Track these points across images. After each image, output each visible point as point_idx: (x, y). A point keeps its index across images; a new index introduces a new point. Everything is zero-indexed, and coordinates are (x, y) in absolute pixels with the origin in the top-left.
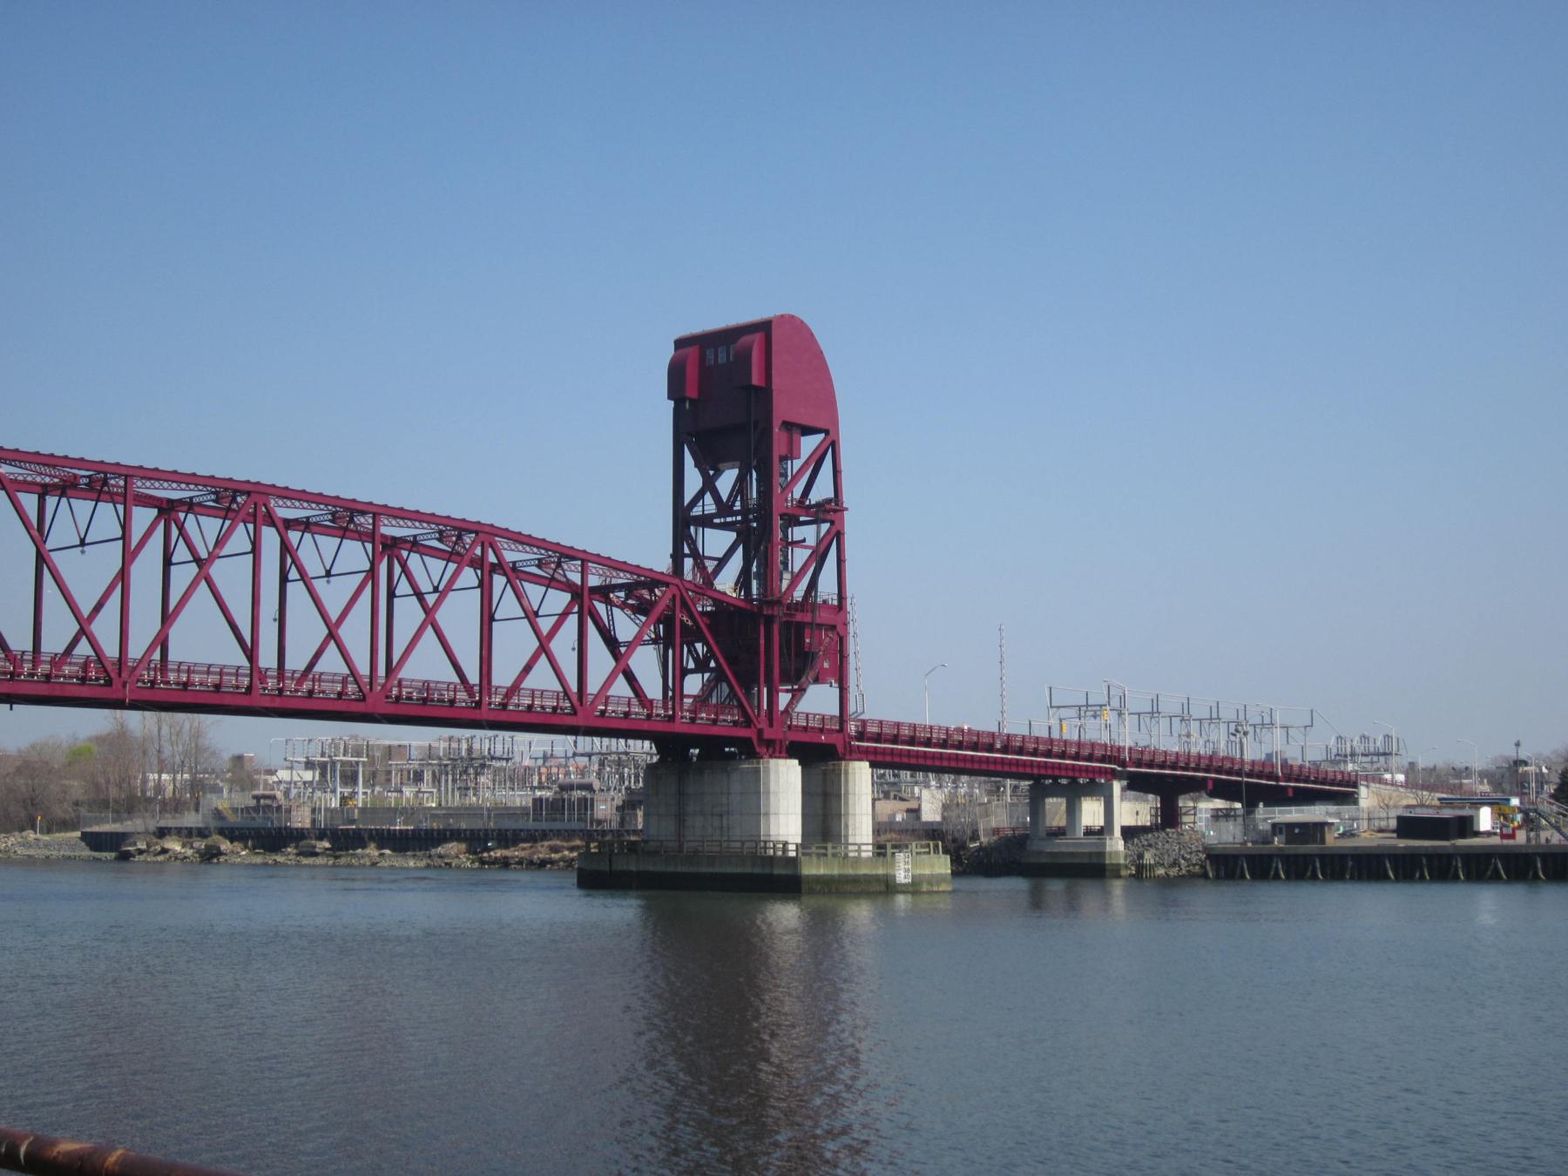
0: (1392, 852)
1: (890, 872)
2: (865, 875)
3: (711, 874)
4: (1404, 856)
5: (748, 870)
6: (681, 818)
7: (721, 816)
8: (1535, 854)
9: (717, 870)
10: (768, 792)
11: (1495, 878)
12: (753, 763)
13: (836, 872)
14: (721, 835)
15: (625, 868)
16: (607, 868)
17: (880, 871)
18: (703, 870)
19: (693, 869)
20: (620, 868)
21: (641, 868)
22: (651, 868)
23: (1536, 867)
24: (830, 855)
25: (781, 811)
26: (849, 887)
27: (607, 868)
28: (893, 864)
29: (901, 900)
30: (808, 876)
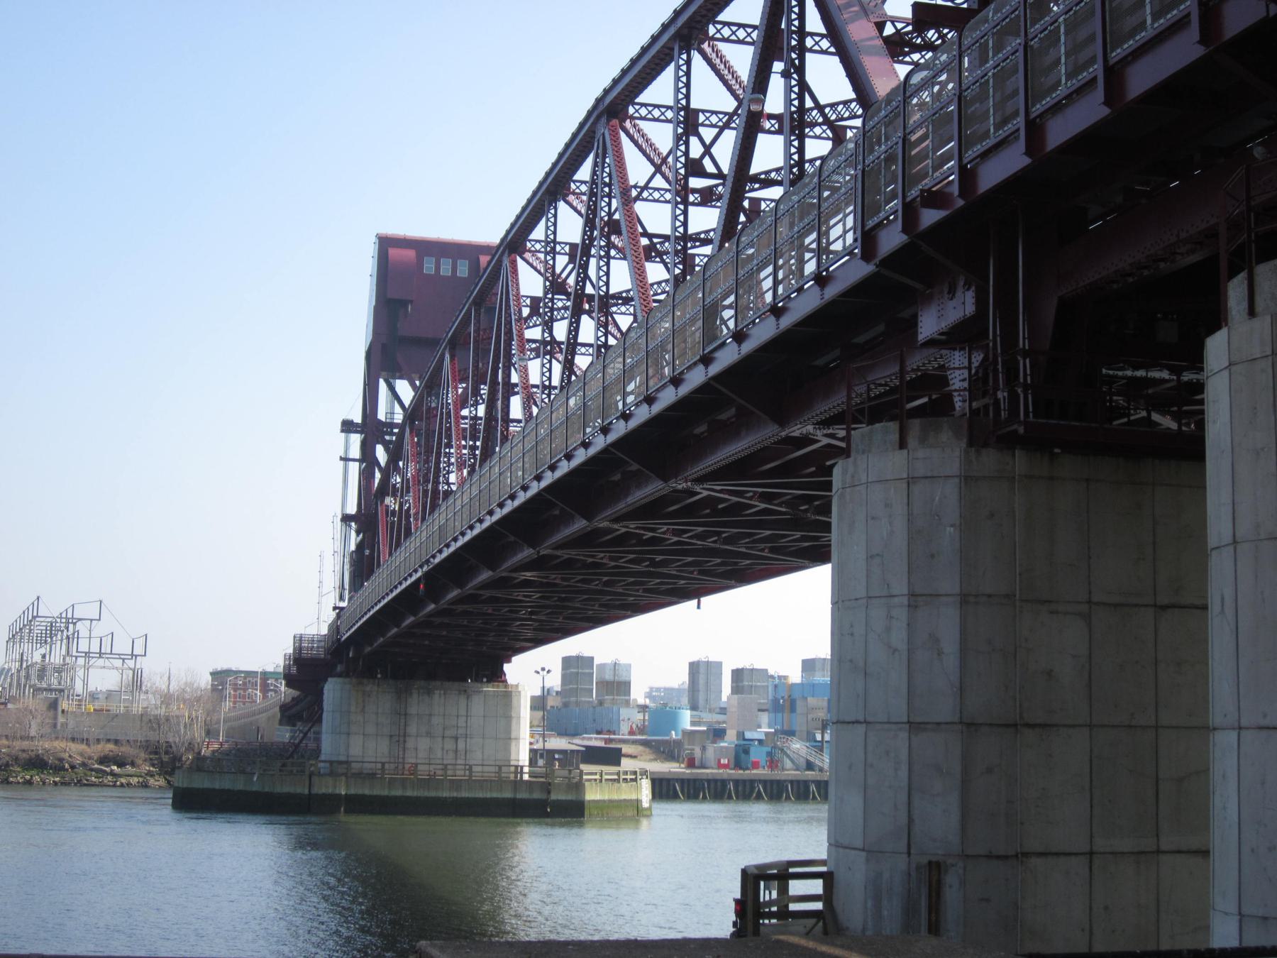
0: (681, 777)
1: (640, 798)
2: (625, 800)
3: (455, 799)
4: (689, 780)
5: (507, 794)
6: (399, 739)
7: (456, 739)
8: (785, 781)
9: (465, 794)
10: (519, 718)
11: (759, 797)
12: (498, 687)
13: (606, 797)
14: (456, 759)
15: (330, 791)
16: (306, 792)
17: (634, 797)
18: (446, 794)
19: (433, 794)
20: (324, 791)
21: (352, 791)
22: (367, 792)
23: (787, 790)
24: (621, 780)
25: (521, 737)
26: (616, 813)
27: (306, 792)
28: (638, 789)
29: (644, 822)
30: (589, 801)
